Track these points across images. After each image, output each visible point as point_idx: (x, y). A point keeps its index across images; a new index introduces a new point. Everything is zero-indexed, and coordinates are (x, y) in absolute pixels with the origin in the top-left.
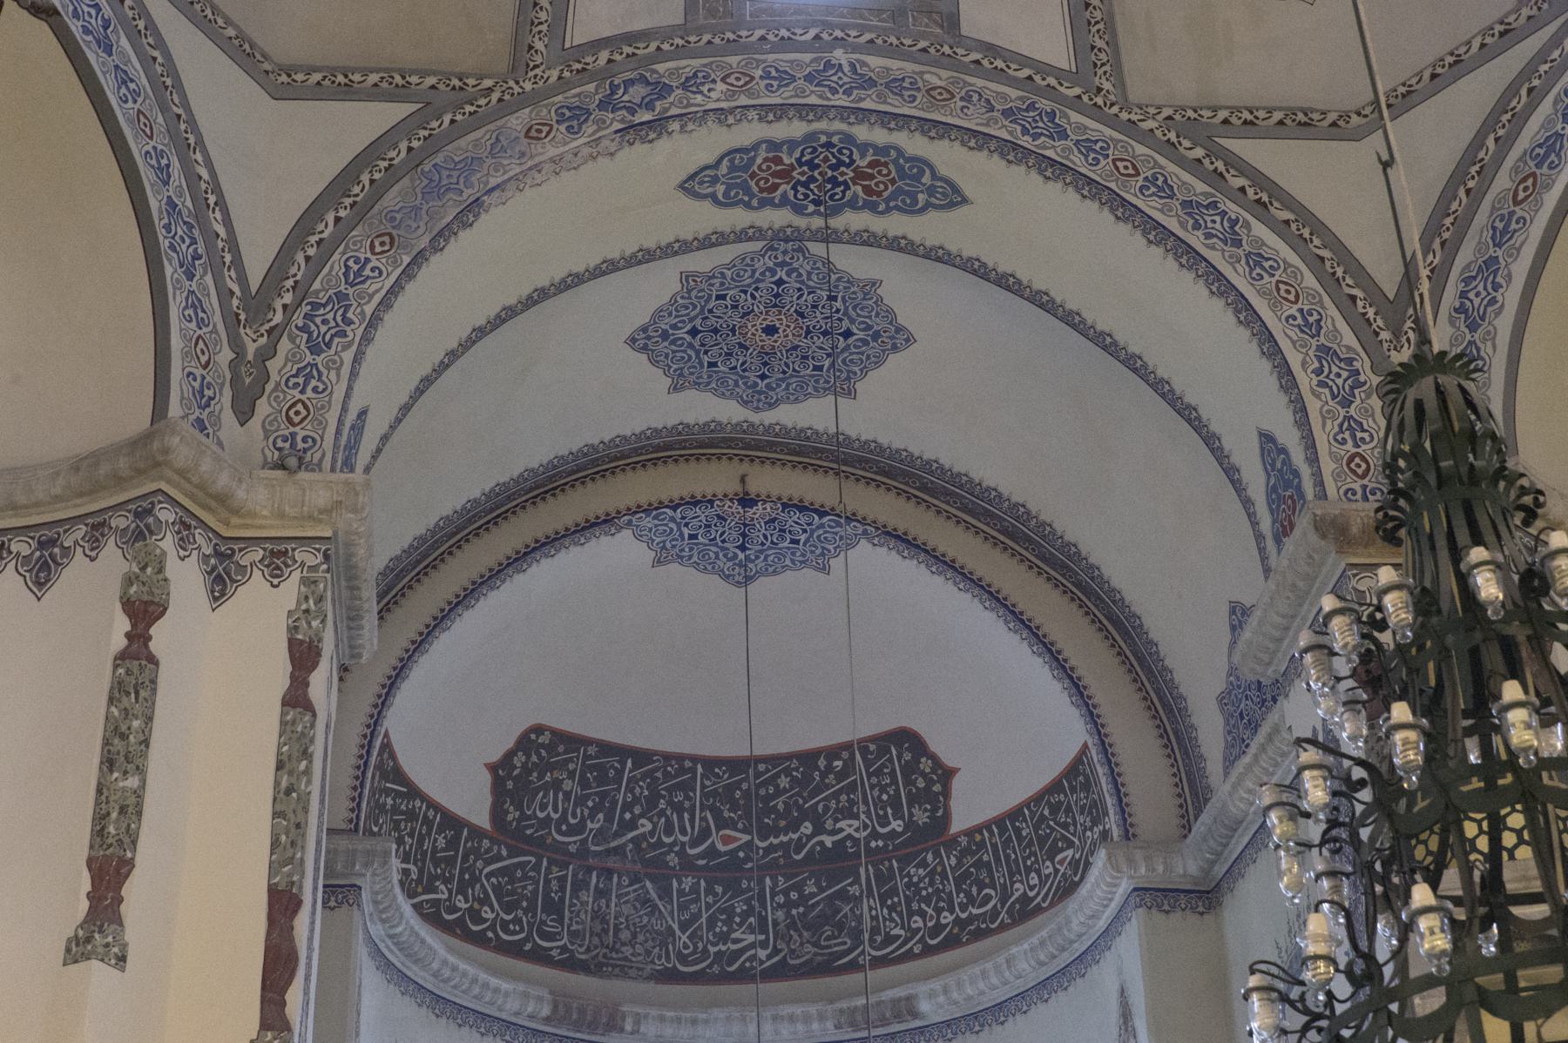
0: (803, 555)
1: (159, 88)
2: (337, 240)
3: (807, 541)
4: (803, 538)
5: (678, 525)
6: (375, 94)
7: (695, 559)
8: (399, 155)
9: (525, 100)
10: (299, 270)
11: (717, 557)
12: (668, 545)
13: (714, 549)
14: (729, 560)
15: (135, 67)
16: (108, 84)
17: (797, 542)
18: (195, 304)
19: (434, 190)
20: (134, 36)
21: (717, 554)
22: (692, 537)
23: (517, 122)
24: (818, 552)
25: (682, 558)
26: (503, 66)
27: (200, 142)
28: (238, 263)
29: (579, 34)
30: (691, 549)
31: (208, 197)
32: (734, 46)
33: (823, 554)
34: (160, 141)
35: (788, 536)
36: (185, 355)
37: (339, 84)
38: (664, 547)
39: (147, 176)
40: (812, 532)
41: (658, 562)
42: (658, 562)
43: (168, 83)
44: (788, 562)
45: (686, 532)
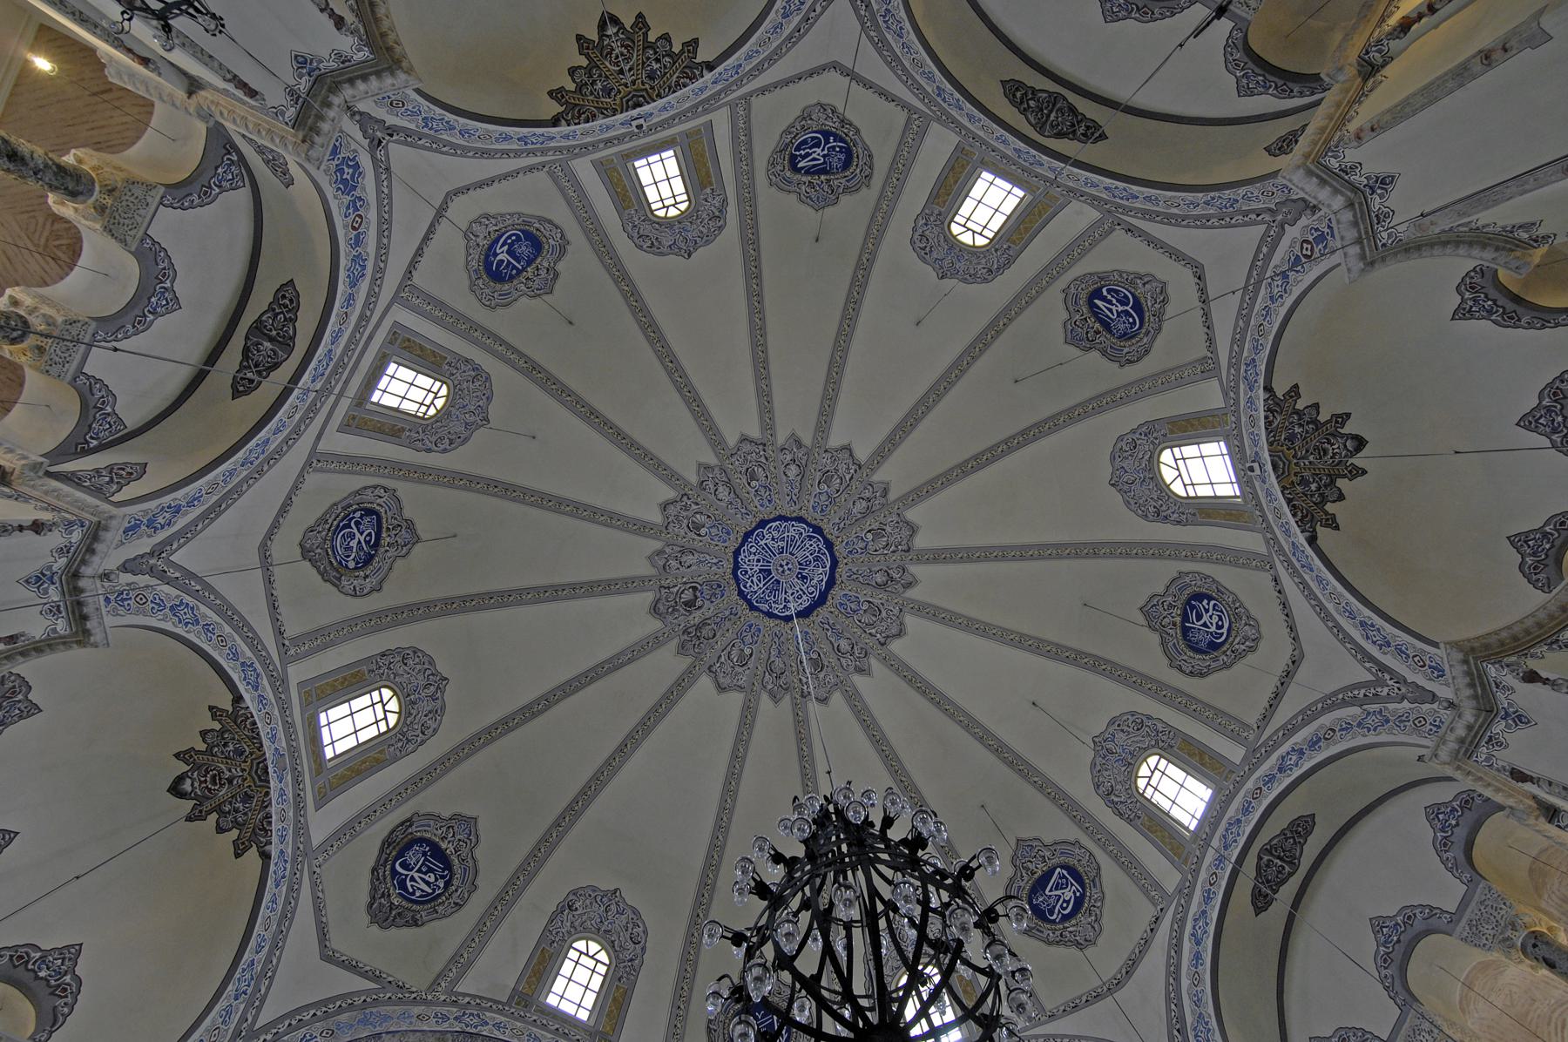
1: (284, 916)
2: (308, 1023)
6: (364, 975)
8: (358, 1001)
9: (425, 1002)
10: (282, 1028)
15: (281, 901)
16: (267, 897)
18: (228, 1012)
19: (364, 1022)
20: (290, 889)
23: (416, 1010)
26: (424, 987)
27: (283, 948)
28: (259, 1009)
29: (460, 988)
31: (268, 973)
32: (522, 1018)
34: (268, 935)
36: (207, 1030)
37: (352, 967)
39: (253, 943)
43: (287, 916)
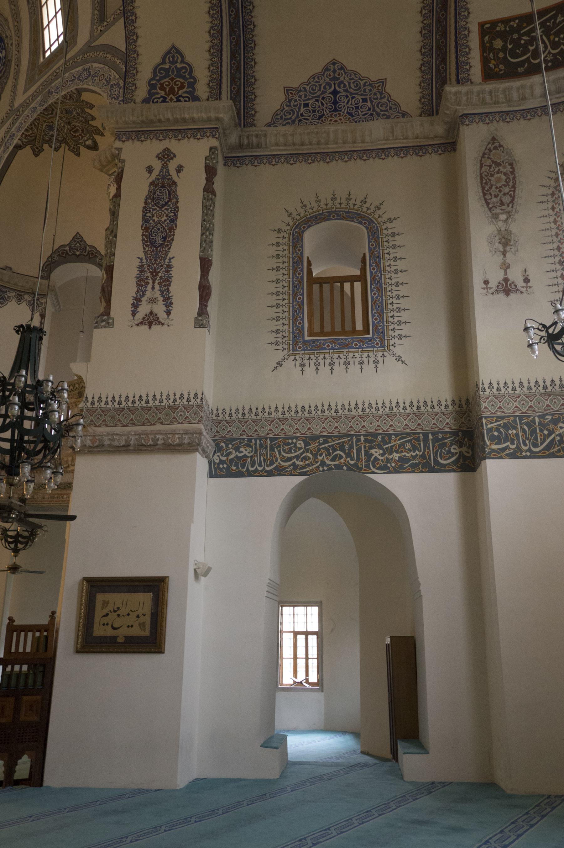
0: (300, 96)
3: (299, 108)
4: (302, 110)
5: (374, 110)
7: (362, 83)
11: (349, 83)
12: (378, 95)
13: (351, 90)
14: (342, 82)
17: (306, 105)
21: (350, 87)
22: (365, 100)
24: (292, 103)
25: (370, 85)
30: (365, 91)
33: (290, 101)
35: (310, 108)
38: (381, 93)
40: (298, 117)
41: (383, 82)
42: (383, 82)
44: (307, 87)
45: (369, 104)
